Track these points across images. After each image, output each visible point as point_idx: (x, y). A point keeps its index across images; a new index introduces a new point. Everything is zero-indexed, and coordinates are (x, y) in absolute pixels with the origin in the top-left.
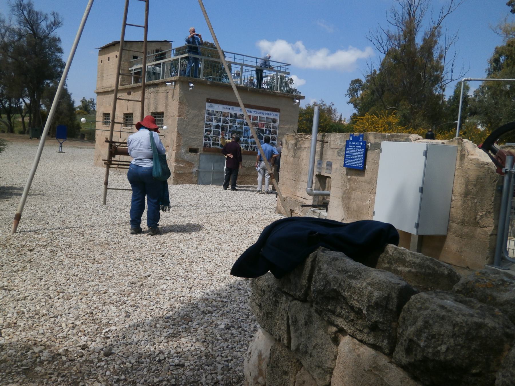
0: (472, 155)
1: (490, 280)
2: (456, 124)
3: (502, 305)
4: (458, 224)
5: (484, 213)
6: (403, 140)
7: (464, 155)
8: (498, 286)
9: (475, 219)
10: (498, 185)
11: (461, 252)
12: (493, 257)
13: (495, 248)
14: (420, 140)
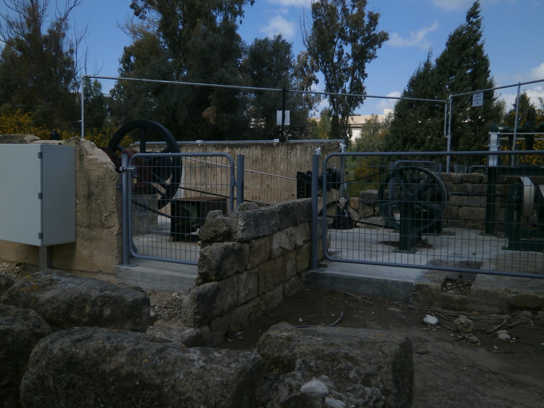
0: (91, 155)
1: (38, 281)
2: (81, 123)
3: (43, 305)
4: (86, 228)
5: (108, 213)
6: (17, 141)
7: (83, 155)
8: (44, 286)
9: (101, 221)
10: (117, 185)
11: (92, 257)
12: (122, 256)
13: (122, 247)
14: (37, 141)
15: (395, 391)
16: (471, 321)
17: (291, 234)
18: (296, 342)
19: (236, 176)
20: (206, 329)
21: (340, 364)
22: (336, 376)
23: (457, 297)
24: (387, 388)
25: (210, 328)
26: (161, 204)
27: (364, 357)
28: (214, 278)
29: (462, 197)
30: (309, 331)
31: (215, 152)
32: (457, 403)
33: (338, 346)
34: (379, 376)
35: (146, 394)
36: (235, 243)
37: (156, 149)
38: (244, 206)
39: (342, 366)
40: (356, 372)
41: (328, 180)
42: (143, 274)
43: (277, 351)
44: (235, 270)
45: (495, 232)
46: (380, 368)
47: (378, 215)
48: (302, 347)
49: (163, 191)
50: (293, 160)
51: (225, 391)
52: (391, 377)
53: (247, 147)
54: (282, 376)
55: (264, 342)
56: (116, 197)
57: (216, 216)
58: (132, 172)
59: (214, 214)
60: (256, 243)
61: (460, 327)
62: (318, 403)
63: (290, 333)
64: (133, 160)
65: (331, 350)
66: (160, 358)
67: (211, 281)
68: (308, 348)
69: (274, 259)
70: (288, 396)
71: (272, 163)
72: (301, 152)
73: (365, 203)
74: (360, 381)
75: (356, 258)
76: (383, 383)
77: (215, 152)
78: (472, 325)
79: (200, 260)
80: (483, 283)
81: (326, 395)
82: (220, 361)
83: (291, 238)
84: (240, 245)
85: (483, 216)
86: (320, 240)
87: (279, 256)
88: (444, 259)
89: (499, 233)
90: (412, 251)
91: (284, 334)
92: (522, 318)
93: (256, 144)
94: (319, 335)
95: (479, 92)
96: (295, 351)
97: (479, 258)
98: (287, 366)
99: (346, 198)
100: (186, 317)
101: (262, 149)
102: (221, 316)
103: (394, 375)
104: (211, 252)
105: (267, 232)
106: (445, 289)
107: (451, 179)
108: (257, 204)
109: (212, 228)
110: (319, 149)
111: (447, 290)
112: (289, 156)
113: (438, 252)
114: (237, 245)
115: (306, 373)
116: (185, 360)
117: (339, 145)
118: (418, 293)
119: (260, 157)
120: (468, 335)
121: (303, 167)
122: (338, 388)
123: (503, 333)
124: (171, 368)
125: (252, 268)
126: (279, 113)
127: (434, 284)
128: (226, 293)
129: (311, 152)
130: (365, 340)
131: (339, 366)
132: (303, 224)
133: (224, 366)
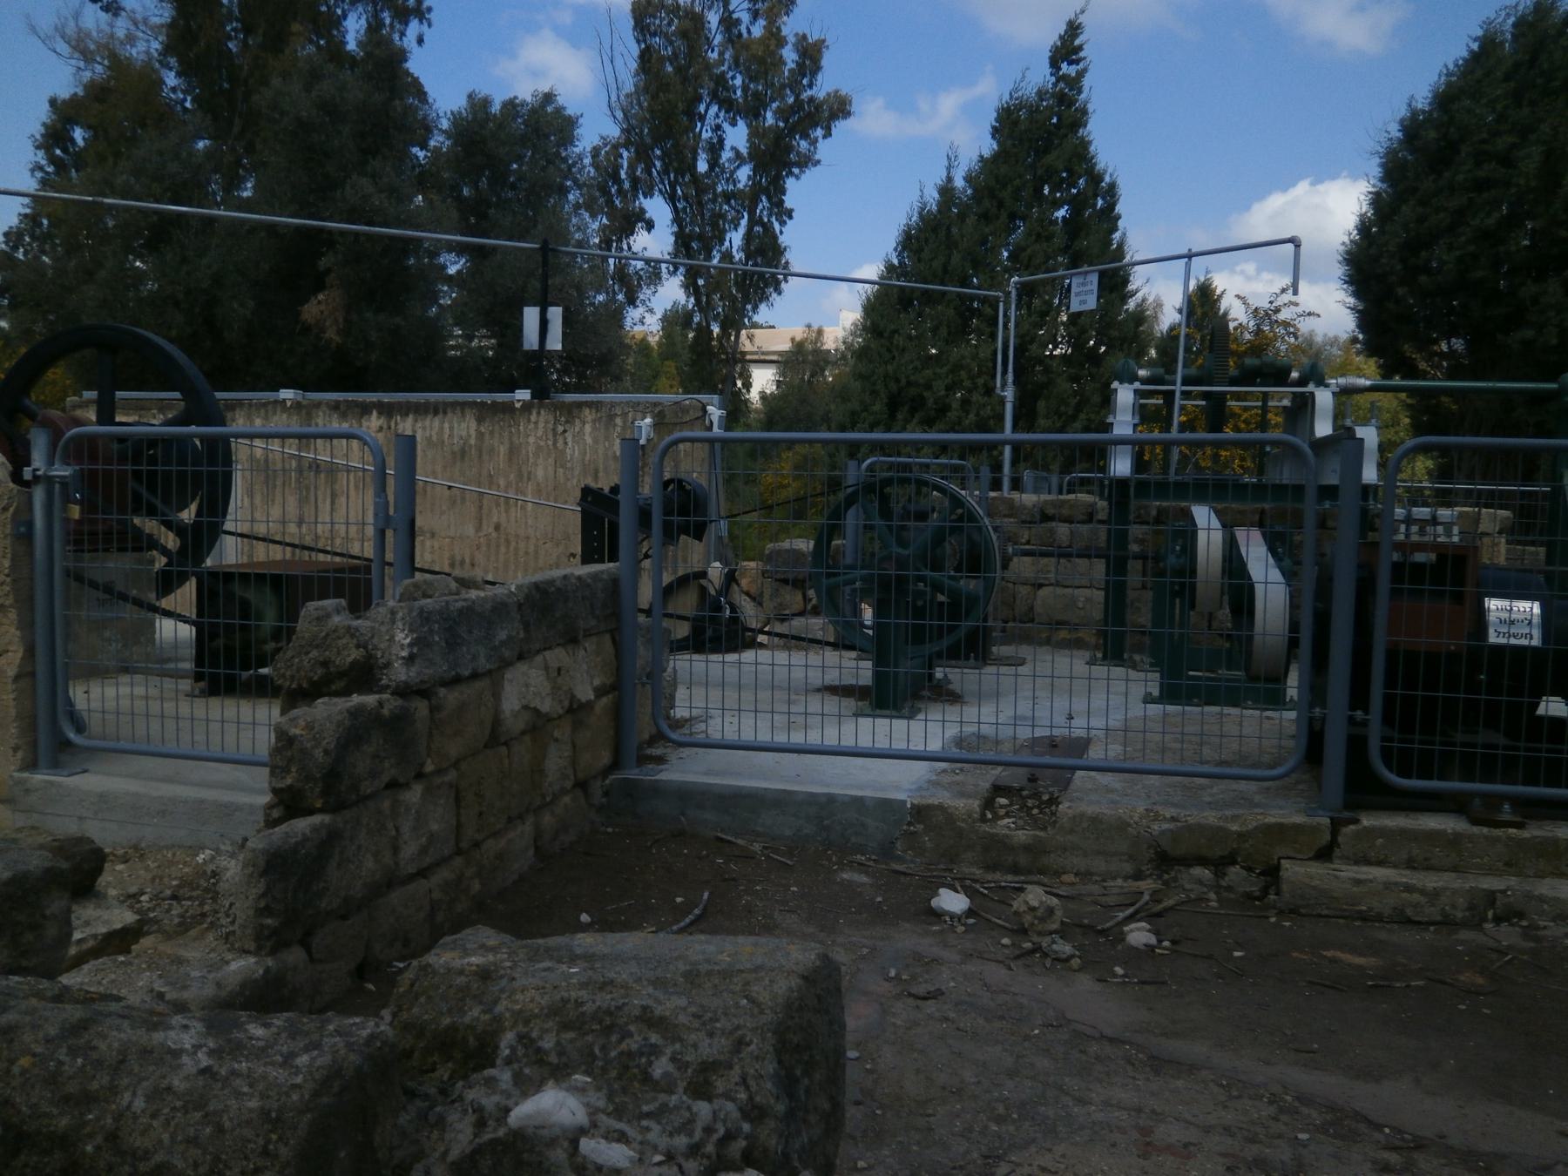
12: (34, 744)
15: (780, 1108)
16: (1055, 901)
17: (559, 670)
18: (504, 982)
19: (391, 498)
20: (295, 955)
21: (628, 1041)
22: (614, 1074)
23: (1022, 836)
24: (758, 1099)
25: (309, 953)
26: (167, 583)
27: (696, 1016)
28: (318, 805)
29: (1046, 560)
30: (547, 950)
31: (336, 425)
32: (1011, 1128)
33: (625, 986)
34: (737, 1068)
35: (26, 1165)
36: (385, 696)
37: (147, 415)
38: (416, 586)
39: (633, 1044)
40: (673, 1059)
41: (667, 511)
42: (103, 797)
43: (450, 1011)
44: (385, 778)
45: (1126, 656)
46: (740, 1044)
47: (816, 612)
48: (519, 997)
49: (171, 541)
50: (573, 451)
51: (274, 1137)
52: (770, 1067)
53: (436, 413)
54: (460, 1084)
55: (412, 985)
56: (12, 560)
57: (328, 616)
58: (64, 482)
59: (321, 613)
60: (450, 698)
61: (1028, 919)
62: (559, 1155)
63: (491, 958)
64: (67, 442)
65: (604, 1000)
66: (73, 1052)
67: (311, 812)
68: (538, 998)
69: (506, 744)
70: (471, 1142)
71: (510, 459)
72: (594, 429)
73: (779, 576)
74: (682, 1085)
75: (748, 736)
76: (747, 1088)
77: (336, 425)
78: (1059, 913)
79: (276, 751)
80: (1090, 795)
81: (582, 1131)
82: (263, 1049)
83: (559, 680)
84: (399, 702)
85: (1098, 615)
86: (643, 685)
87: (523, 733)
88: (986, 730)
89: (1137, 658)
90: (906, 711)
91: (473, 960)
92: (1188, 886)
93: (463, 405)
94: (573, 959)
95: (1086, 273)
96: (499, 1008)
97: (1078, 729)
98: (474, 1053)
99: (725, 563)
100: (233, 923)
101: (480, 420)
102: (344, 917)
103: (780, 1062)
104: (309, 727)
105: (483, 664)
106: (989, 816)
107: (1012, 509)
108: (457, 580)
109: (314, 653)
110: (648, 420)
111: (996, 817)
112: (560, 444)
113: (970, 712)
114: (391, 704)
115: (527, 1071)
116: (151, 1052)
117: (705, 411)
118: (920, 827)
119: (473, 442)
120: (1048, 939)
121: (601, 474)
122: (616, 1110)
123: (1138, 929)
124: (106, 1080)
125: (439, 772)
126: (531, 315)
127: (960, 803)
128: (359, 847)
129: (624, 428)
130: (704, 968)
131: (624, 1046)
132: (594, 639)
133: (273, 1064)
